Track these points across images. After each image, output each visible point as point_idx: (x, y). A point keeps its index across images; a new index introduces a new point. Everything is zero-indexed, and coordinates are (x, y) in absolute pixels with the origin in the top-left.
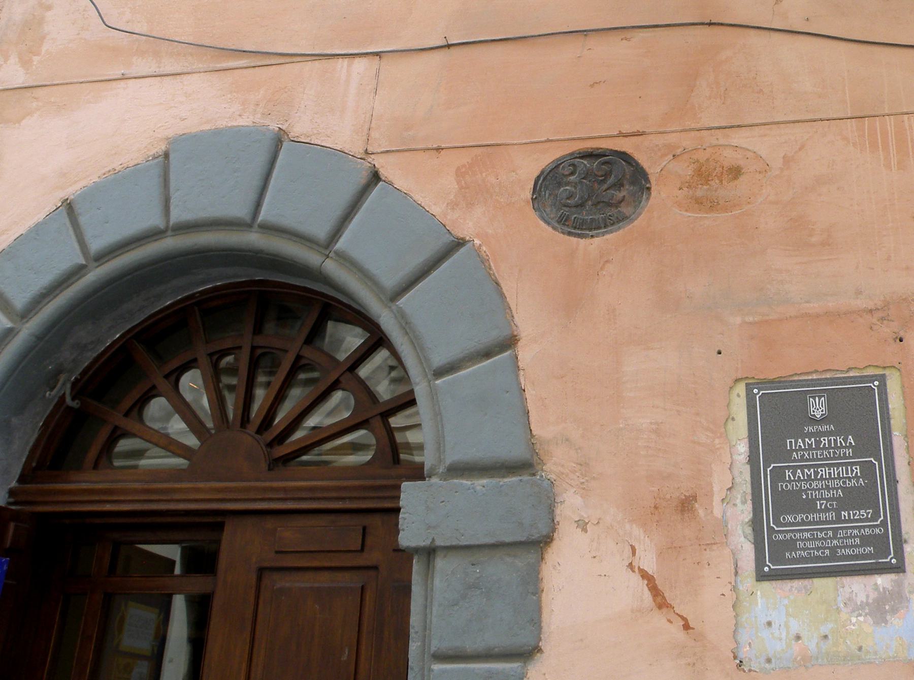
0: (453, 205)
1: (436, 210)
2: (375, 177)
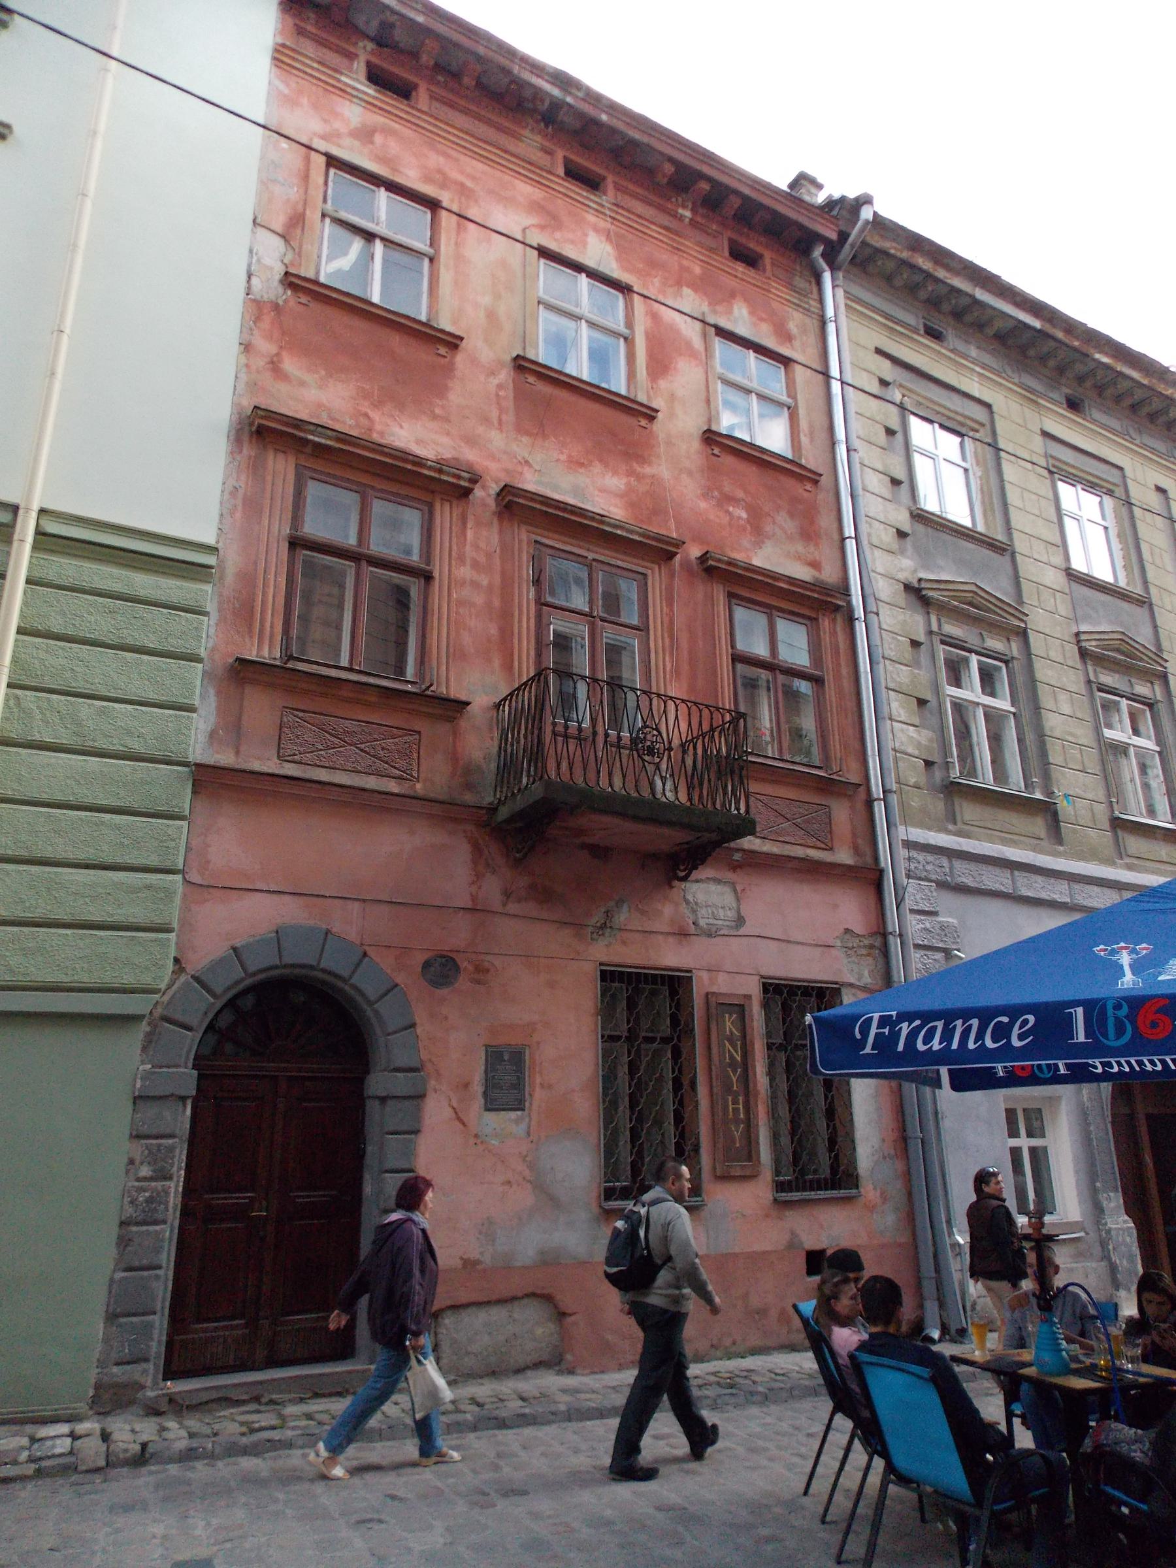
1: (389, 971)
2: (365, 954)
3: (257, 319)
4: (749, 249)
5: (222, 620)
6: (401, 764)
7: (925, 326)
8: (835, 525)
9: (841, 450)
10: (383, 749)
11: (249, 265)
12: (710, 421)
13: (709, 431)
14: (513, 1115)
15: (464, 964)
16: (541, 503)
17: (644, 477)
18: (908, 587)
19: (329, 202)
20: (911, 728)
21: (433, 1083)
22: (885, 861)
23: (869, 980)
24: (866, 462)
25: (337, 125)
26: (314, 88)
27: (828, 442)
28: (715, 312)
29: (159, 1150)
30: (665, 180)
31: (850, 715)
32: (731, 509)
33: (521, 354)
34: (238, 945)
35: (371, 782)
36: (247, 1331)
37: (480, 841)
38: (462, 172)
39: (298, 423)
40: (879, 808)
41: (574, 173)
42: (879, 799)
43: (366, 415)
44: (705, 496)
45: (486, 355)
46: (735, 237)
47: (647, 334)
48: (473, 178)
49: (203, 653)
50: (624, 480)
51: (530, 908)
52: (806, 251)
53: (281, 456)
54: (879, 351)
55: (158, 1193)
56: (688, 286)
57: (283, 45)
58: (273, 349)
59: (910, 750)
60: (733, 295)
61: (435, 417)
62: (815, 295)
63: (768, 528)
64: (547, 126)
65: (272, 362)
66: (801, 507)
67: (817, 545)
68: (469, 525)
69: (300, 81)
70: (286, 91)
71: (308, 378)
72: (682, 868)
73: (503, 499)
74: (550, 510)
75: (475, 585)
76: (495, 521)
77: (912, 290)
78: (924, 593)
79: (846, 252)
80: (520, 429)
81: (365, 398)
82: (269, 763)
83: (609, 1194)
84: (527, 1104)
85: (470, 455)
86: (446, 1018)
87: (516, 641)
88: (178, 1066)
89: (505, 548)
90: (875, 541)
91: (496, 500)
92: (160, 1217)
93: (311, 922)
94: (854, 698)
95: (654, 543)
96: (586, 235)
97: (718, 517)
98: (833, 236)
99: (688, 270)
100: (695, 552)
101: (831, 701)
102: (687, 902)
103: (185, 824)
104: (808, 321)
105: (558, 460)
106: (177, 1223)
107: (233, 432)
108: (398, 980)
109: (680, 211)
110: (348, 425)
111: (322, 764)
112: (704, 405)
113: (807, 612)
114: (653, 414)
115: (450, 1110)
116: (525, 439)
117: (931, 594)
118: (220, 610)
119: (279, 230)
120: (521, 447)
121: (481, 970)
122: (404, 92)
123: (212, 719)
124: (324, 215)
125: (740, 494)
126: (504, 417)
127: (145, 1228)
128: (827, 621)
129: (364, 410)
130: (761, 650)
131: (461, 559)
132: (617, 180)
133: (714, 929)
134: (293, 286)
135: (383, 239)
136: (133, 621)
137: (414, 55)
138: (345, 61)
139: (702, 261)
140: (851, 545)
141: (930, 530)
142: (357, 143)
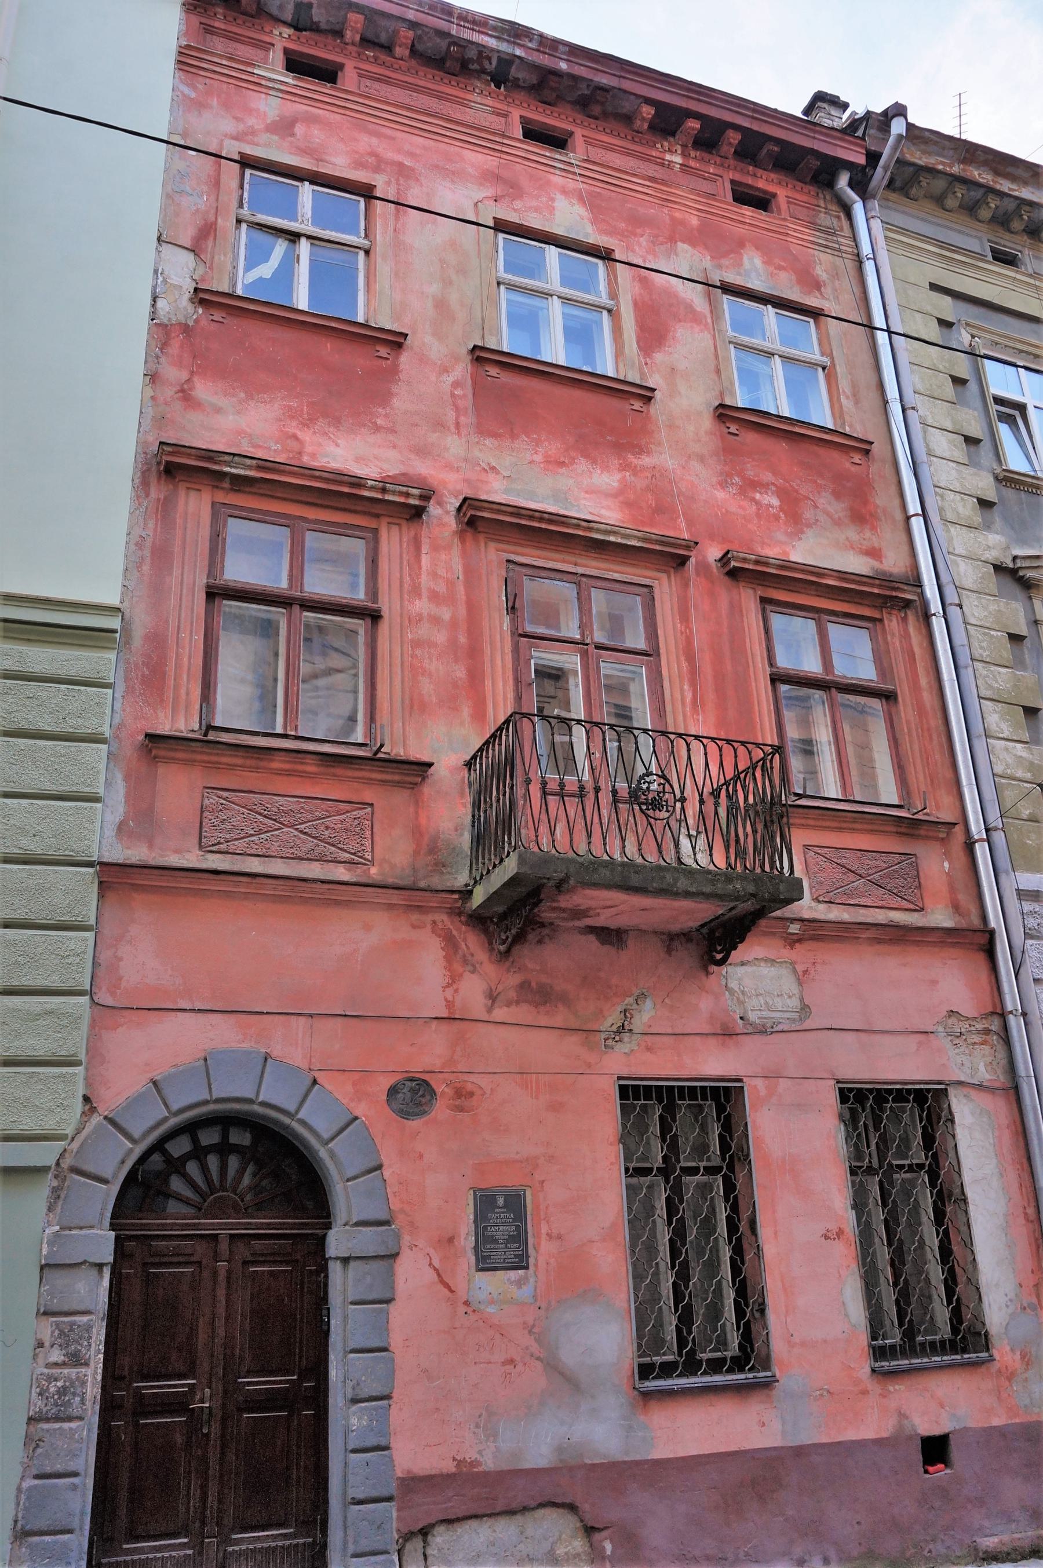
0: (352, 1100)
1: (344, 1101)
2: (315, 1082)
3: (164, 345)
4: (758, 189)
5: (129, 690)
6: (352, 845)
7: (993, 251)
8: (897, 502)
9: (895, 408)
10: (327, 828)
11: (154, 287)
12: (722, 394)
13: (722, 406)
14: (513, 1275)
15: (440, 1088)
16: (512, 514)
17: (643, 469)
18: (998, 568)
19: (246, 206)
20: (1019, 746)
21: (406, 1239)
22: (995, 920)
23: (988, 1077)
24: (930, 421)
25: (252, 121)
26: (225, 86)
27: (878, 402)
28: (720, 267)
29: (71, 1330)
30: (646, 126)
31: (935, 737)
32: (758, 496)
33: (480, 344)
34: (158, 1078)
35: (314, 870)
36: (190, 1552)
37: (455, 933)
38: (399, 151)
39: (210, 455)
40: (981, 851)
41: (533, 134)
42: (982, 840)
43: (295, 437)
44: (723, 485)
45: (436, 350)
46: (738, 177)
47: (635, 304)
48: (411, 155)
49: (107, 731)
50: (618, 476)
51: (523, 1013)
52: (830, 184)
53: (193, 494)
54: (934, 287)
55: (72, 1383)
56: (684, 242)
57: (188, 47)
58: (184, 375)
59: (1019, 774)
60: (741, 244)
61: (377, 429)
62: (847, 231)
63: (808, 514)
64: (498, 87)
65: (182, 391)
66: (849, 485)
67: (874, 528)
68: (424, 551)
69: (208, 81)
70: (193, 95)
71: (222, 402)
72: (719, 948)
73: (465, 514)
74: (523, 522)
75: (435, 620)
76: (456, 540)
77: (971, 209)
78: (1021, 574)
79: (880, 176)
80: (483, 431)
81: (292, 417)
82: (188, 856)
83: (645, 1371)
84: (531, 1261)
85: (422, 468)
86: (421, 1156)
87: (488, 683)
88: (92, 1227)
89: (471, 574)
90: (950, 516)
91: (456, 517)
92: (76, 1412)
93: (246, 1045)
94: (939, 714)
95: (658, 548)
96: (553, 200)
97: (741, 507)
98: (861, 160)
99: (682, 223)
100: (713, 553)
101: (908, 722)
102: (732, 992)
103: (90, 935)
104: (838, 261)
105: (532, 462)
106: (96, 1420)
107: (139, 474)
108: (357, 1112)
109: (668, 157)
110: (275, 452)
111: (252, 851)
112: (714, 376)
113: (867, 612)
114: (649, 394)
115: (432, 1271)
116: (489, 442)
117: (1030, 574)
118: (127, 679)
119: (188, 245)
120: (487, 451)
121: (462, 1094)
122: (328, 74)
123: (121, 809)
124: (239, 221)
125: (768, 477)
126: (463, 420)
127: (57, 1425)
128: (894, 623)
129: (291, 431)
130: (811, 665)
131: (416, 591)
132: (586, 133)
133: (769, 1025)
134: (202, 302)
135: (309, 237)
136: (27, 702)
137: (338, 33)
138: (261, 53)
139: (699, 210)
140: (917, 525)
141: (1023, 494)
142: (275, 138)
